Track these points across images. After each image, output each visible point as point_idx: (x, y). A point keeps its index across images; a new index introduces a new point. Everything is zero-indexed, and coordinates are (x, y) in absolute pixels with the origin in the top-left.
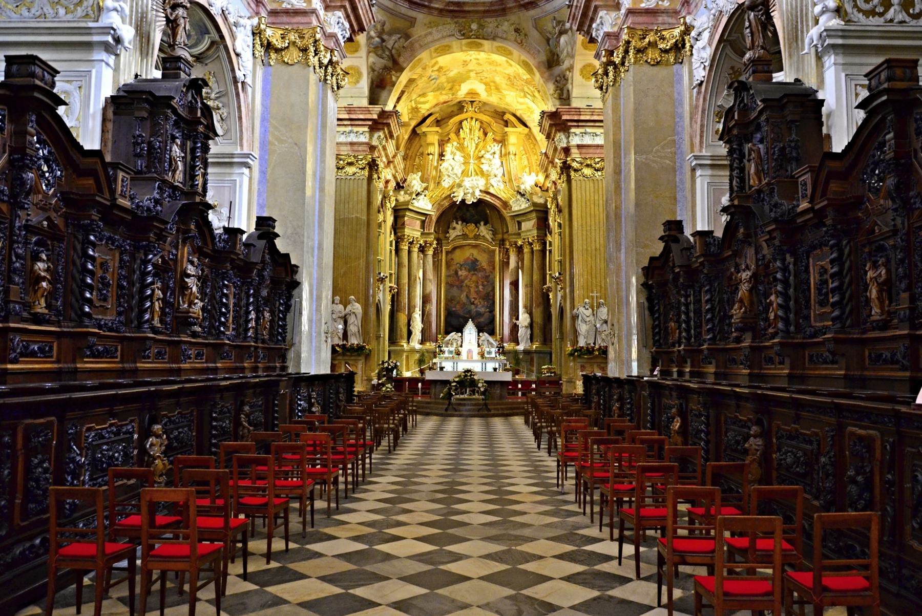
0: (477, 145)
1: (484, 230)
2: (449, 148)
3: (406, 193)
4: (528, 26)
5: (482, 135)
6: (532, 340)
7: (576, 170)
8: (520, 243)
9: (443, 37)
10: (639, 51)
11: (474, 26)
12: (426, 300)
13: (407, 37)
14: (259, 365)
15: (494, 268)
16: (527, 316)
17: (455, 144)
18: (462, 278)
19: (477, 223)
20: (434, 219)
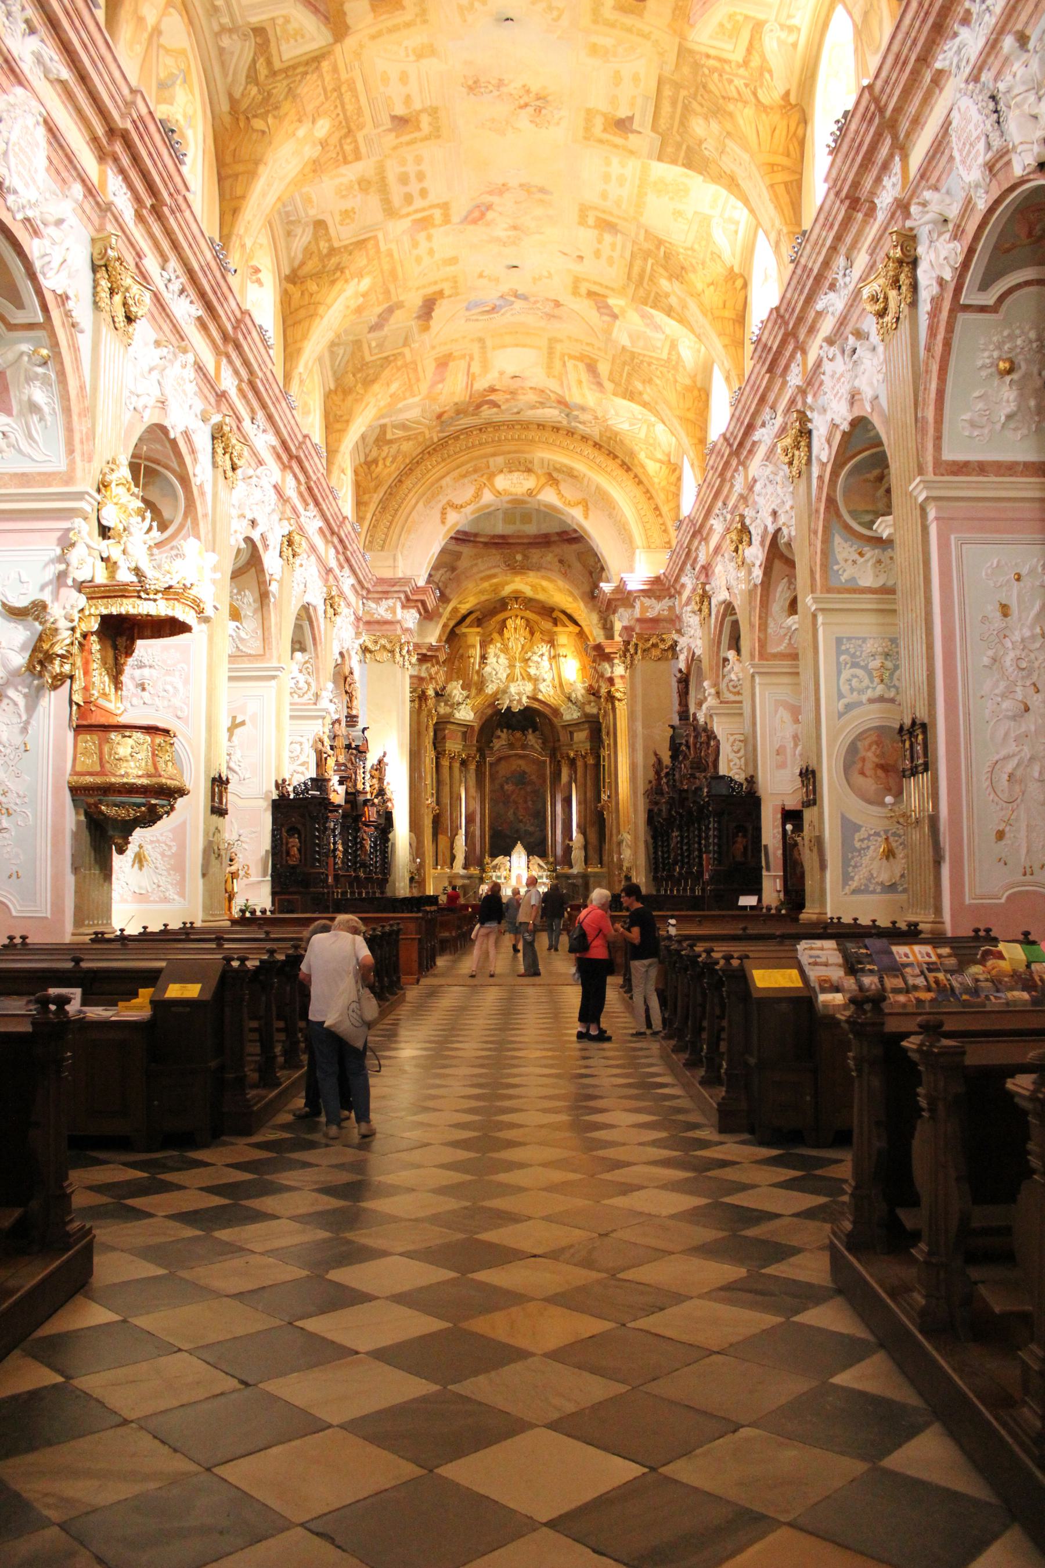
0: (523, 646)
1: (532, 738)
2: (492, 650)
4: (573, 559)
5: (528, 636)
8: (572, 755)
9: (490, 568)
10: (644, 651)
11: (519, 557)
12: (470, 820)
13: (453, 569)
15: (545, 782)
16: (581, 837)
17: (499, 645)
19: (523, 730)
20: (477, 729)
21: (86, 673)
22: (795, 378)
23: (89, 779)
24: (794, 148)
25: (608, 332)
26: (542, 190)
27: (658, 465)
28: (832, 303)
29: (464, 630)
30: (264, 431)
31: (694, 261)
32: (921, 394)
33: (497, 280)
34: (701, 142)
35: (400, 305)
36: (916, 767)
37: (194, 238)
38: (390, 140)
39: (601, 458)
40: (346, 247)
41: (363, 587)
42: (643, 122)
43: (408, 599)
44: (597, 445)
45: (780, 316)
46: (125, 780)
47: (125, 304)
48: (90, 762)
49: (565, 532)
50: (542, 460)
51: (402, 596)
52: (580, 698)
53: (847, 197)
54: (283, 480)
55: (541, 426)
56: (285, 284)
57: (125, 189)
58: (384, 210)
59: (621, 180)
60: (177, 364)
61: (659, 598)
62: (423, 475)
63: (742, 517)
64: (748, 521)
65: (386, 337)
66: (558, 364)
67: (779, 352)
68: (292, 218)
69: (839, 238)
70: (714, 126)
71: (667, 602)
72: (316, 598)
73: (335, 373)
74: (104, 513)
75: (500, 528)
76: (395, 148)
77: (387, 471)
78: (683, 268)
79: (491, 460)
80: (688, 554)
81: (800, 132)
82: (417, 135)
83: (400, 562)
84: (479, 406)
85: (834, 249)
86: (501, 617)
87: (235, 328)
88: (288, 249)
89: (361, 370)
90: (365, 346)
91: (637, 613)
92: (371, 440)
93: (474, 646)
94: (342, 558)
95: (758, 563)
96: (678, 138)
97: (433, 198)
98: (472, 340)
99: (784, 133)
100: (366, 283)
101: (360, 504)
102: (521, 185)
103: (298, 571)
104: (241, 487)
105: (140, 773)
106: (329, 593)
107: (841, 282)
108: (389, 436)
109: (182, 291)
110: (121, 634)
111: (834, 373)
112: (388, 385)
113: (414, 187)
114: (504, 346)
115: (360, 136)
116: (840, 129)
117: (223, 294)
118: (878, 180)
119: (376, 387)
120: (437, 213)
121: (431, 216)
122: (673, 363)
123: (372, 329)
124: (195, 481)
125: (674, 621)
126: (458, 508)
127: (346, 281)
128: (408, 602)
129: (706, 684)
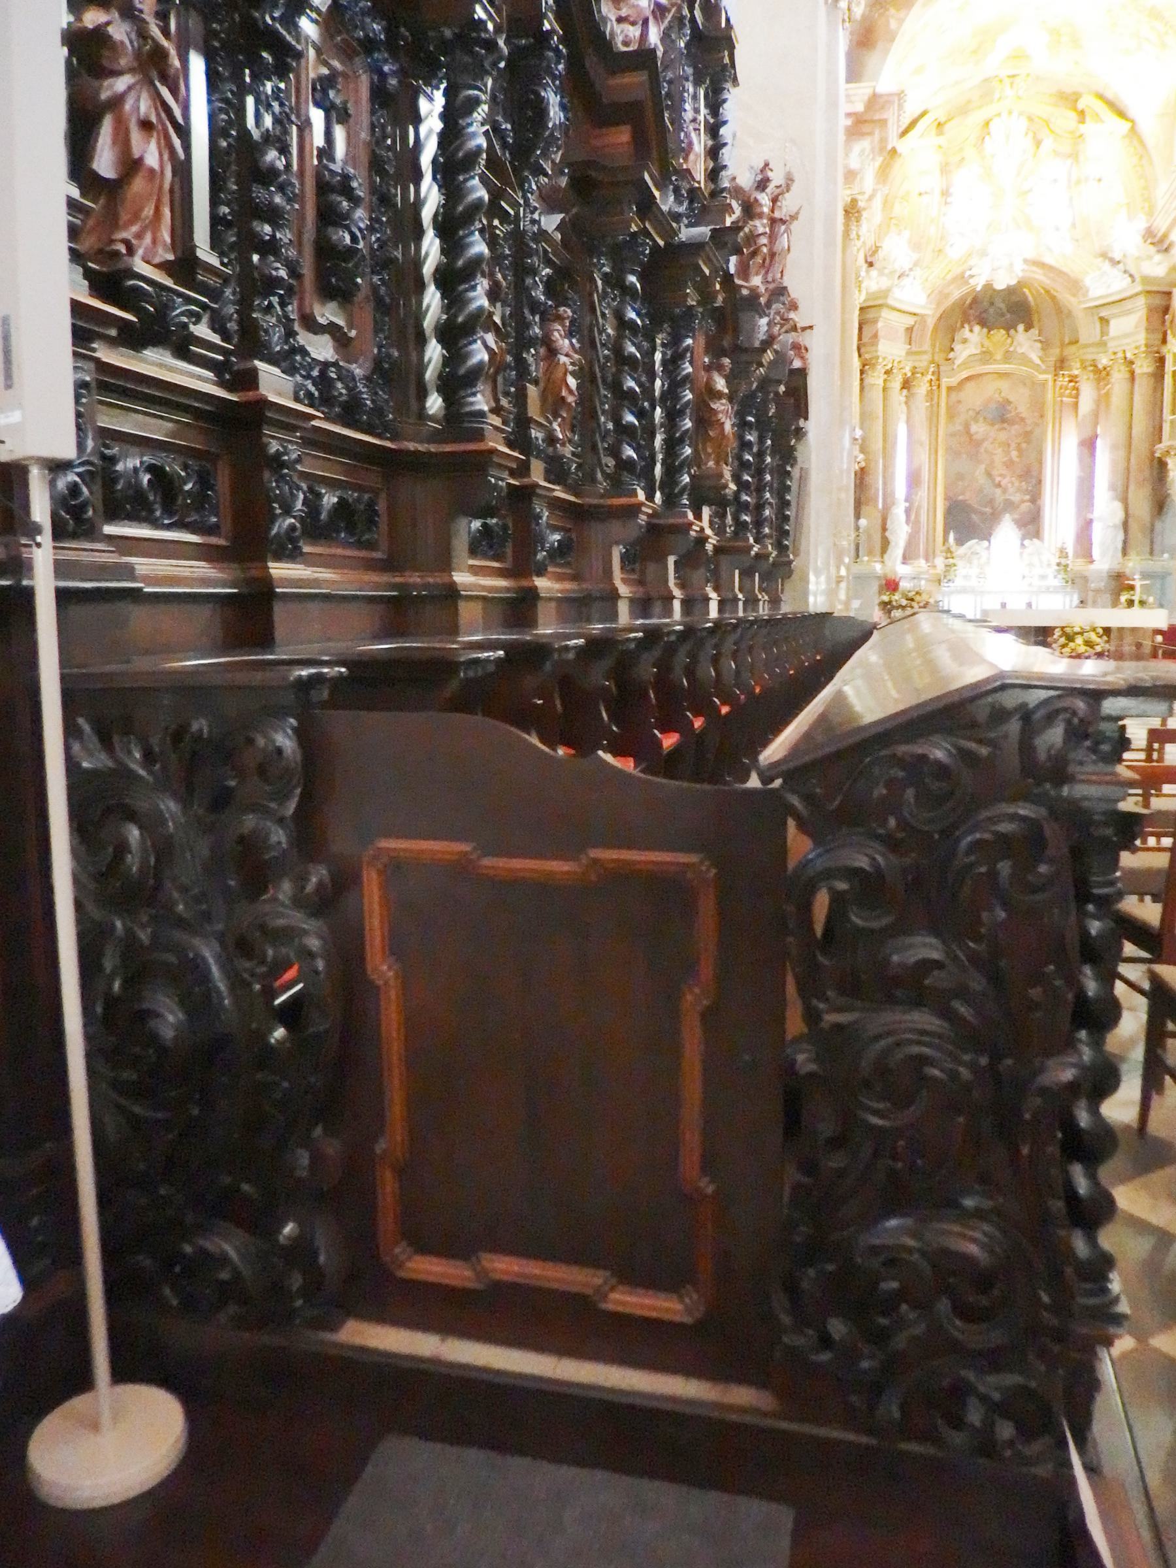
1: (1025, 342)
3: (881, 274)
12: (913, 481)
14: (542, 583)
18: (978, 437)
20: (931, 323)
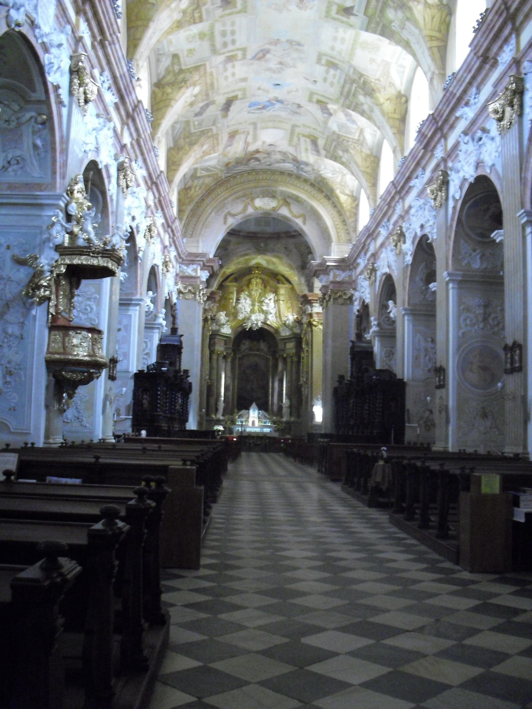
0: (260, 294)
1: (263, 346)
2: (242, 296)
3: (217, 325)
6: (291, 415)
7: (315, 326)
8: (285, 355)
16: (288, 400)
17: (247, 293)
21: (57, 297)
22: (439, 153)
23: (57, 356)
24: (443, 28)
25: (326, 123)
26: (299, 44)
27: (346, 197)
28: (467, 113)
29: (229, 284)
30: (141, 168)
31: (379, 87)
32: (524, 164)
33: (267, 91)
34: (391, 22)
35: (213, 102)
36: (515, 368)
37: (119, 59)
38: (219, 12)
39: (314, 192)
40: (188, 69)
41: (180, 257)
42: (359, 10)
43: (204, 265)
44: (312, 185)
45: (434, 119)
46: (77, 358)
47: (85, 93)
48: (57, 346)
49: (289, 232)
50: (282, 192)
51: (201, 263)
52: (291, 324)
53: (482, 56)
54: (147, 195)
55: (282, 173)
56: (154, 88)
57: (88, 30)
58: (212, 50)
59: (343, 40)
60: (105, 129)
61: (344, 270)
62: (216, 197)
63: (401, 227)
64: (404, 230)
65: (203, 120)
66: (295, 139)
67: (432, 138)
68: (160, 52)
69: (474, 78)
70: (400, 14)
71: (348, 273)
72: (159, 261)
73: (174, 138)
74: (70, 208)
75: (253, 228)
76: (221, 17)
77: (196, 193)
78: (373, 90)
79: (254, 190)
80: (363, 247)
81: (447, 19)
82: (235, 10)
83: (201, 245)
84: (249, 160)
85: (470, 84)
86: (248, 278)
87: (133, 110)
88: (157, 67)
89: (188, 137)
90: (192, 124)
91: (331, 277)
92: (188, 176)
93: (233, 293)
94: (171, 240)
95: (410, 253)
96: (378, 19)
97: (238, 45)
98: (250, 124)
99: (439, 19)
100: (197, 90)
101: (180, 211)
102: (288, 41)
103: (152, 246)
104: (129, 197)
105: (85, 354)
106: (165, 260)
107: (472, 101)
108: (199, 174)
109: (109, 88)
110: (76, 275)
111: (467, 151)
112: (202, 146)
113: (229, 38)
114: (267, 128)
115: (204, 9)
116: (482, 18)
117: (130, 91)
118: (501, 48)
119: (196, 147)
120: (240, 54)
121: (236, 55)
122: (361, 142)
123: (196, 115)
124: (109, 194)
125: (352, 284)
126: (233, 215)
127: (187, 88)
128: (204, 267)
129: (372, 318)
